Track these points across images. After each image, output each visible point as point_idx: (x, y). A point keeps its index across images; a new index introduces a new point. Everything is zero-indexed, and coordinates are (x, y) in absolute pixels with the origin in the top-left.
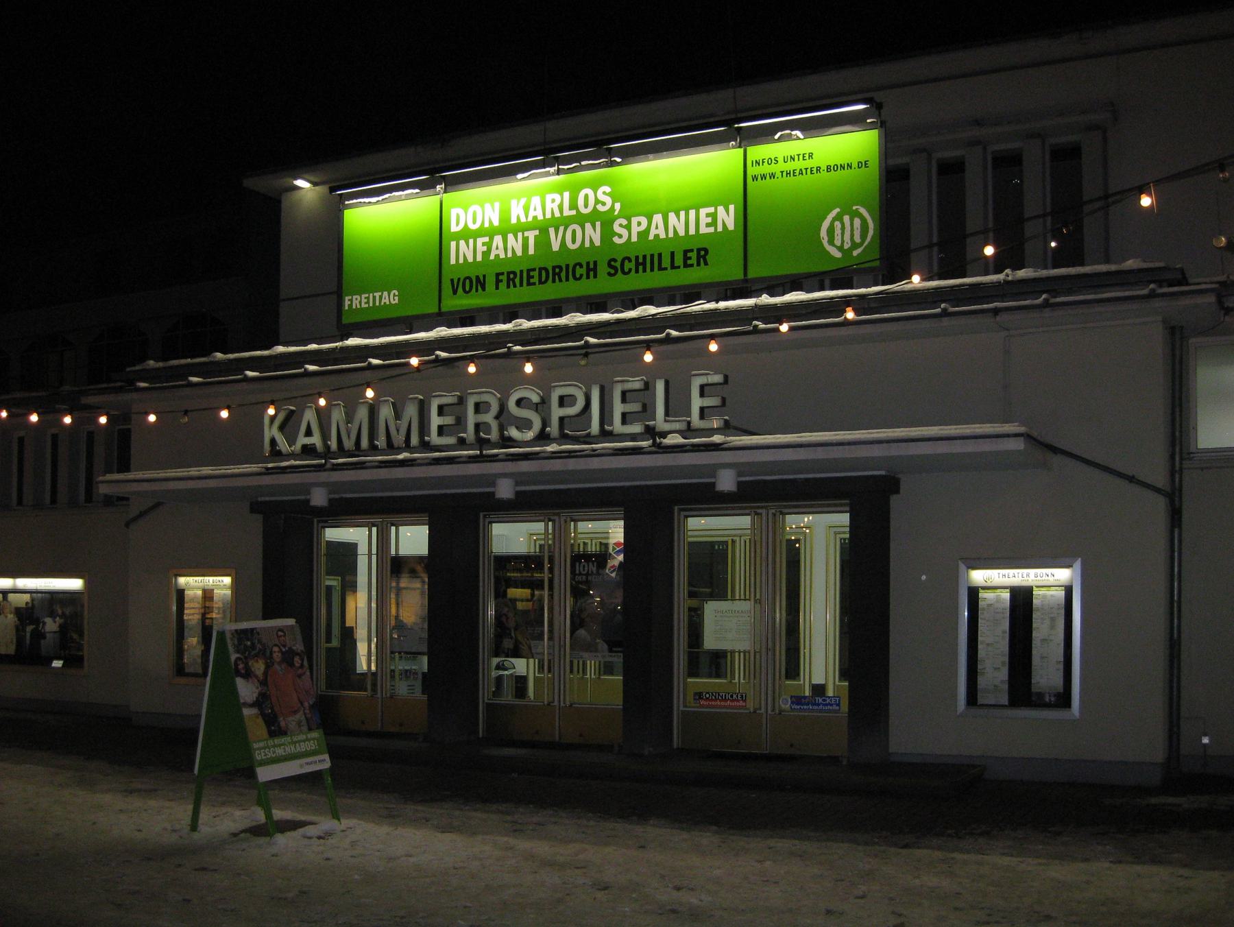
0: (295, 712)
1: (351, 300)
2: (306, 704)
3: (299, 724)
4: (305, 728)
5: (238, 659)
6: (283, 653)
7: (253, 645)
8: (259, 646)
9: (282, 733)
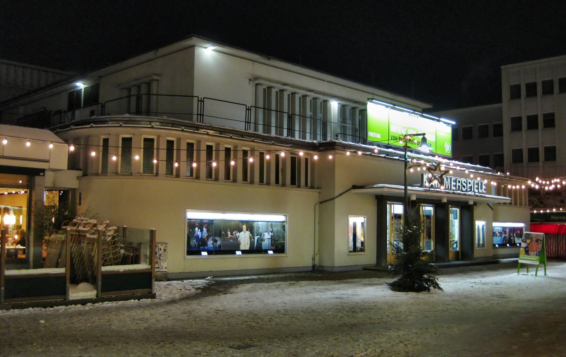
0: (534, 251)
1: (370, 133)
2: (538, 251)
3: (534, 254)
4: (535, 255)
5: (524, 239)
6: (536, 239)
7: (529, 237)
8: (530, 237)
9: (528, 254)
